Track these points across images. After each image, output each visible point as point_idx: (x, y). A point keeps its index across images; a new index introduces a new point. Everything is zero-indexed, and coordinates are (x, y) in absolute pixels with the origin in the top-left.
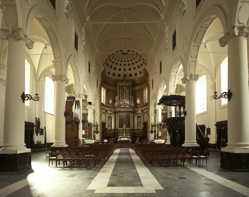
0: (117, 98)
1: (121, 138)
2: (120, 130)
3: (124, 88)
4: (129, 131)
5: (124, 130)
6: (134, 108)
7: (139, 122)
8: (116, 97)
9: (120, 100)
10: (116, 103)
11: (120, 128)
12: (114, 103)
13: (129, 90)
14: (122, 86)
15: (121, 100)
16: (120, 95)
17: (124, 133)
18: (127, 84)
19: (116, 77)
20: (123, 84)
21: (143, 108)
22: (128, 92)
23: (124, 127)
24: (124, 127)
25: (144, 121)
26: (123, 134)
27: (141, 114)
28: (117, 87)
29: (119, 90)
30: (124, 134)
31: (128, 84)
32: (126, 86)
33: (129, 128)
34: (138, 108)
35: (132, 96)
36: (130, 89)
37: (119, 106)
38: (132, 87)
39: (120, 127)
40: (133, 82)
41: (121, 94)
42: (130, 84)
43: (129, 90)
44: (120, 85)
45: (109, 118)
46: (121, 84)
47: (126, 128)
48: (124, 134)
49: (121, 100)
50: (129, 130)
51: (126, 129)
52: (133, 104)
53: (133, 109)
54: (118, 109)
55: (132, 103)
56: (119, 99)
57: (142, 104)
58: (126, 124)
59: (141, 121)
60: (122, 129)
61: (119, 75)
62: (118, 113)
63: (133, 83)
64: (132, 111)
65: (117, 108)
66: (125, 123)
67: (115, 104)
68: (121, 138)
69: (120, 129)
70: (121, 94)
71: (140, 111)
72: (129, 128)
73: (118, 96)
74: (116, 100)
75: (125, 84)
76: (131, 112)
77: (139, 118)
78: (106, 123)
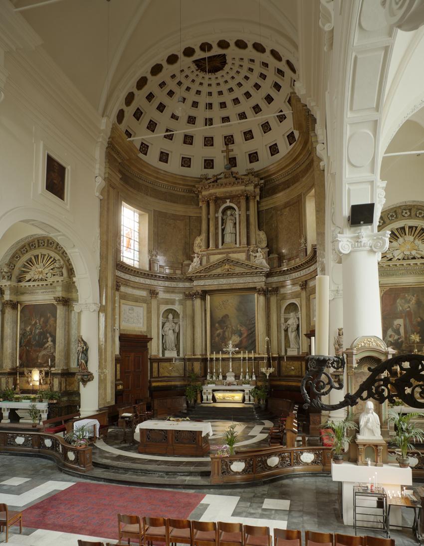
0: (199, 241)
1: (214, 391)
3: (228, 204)
5: (228, 359)
6: (269, 275)
7: (290, 330)
9: (210, 248)
12: (186, 262)
13: (248, 209)
14: (216, 197)
15: (217, 246)
16: (212, 229)
18: (238, 189)
19: (197, 170)
20: (223, 190)
21: (303, 273)
22: (244, 219)
23: (231, 348)
24: (231, 348)
26: (225, 377)
27: (297, 295)
28: (201, 204)
29: (208, 213)
30: (231, 378)
31: (243, 188)
32: (232, 198)
33: (250, 352)
34: (284, 273)
35: (260, 229)
36: (253, 206)
37: (206, 272)
38: (258, 198)
39: (216, 347)
40: (261, 179)
41: (217, 228)
42: (250, 188)
43: (248, 209)
44: (211, 195)
46: (212, 191)
48: (231, 378)
49: (217, 246)
51: (239, 356)
52: (264, 261)
53: (264, 279)
54: (202, 282)
55: (258, 254)
56: (208, 246)
57: (302, 254)
58: (240, 336)
59: (298, 326)
60: (220, 356)
61: (209, 164)
62: (208, 298)
63: (262, 181)
64: (258, 286)
65: (200, 278)
66: (234, 332)
67: (189, 265)
68: (214, 391)
69: (214, 356)
70: (217, 228)
71: (293, 284)
73: (204, 236)
74: (197, 250)
75: (229, 189)
76: (254, 289)
77: (292, 314)
78: (154, 334)
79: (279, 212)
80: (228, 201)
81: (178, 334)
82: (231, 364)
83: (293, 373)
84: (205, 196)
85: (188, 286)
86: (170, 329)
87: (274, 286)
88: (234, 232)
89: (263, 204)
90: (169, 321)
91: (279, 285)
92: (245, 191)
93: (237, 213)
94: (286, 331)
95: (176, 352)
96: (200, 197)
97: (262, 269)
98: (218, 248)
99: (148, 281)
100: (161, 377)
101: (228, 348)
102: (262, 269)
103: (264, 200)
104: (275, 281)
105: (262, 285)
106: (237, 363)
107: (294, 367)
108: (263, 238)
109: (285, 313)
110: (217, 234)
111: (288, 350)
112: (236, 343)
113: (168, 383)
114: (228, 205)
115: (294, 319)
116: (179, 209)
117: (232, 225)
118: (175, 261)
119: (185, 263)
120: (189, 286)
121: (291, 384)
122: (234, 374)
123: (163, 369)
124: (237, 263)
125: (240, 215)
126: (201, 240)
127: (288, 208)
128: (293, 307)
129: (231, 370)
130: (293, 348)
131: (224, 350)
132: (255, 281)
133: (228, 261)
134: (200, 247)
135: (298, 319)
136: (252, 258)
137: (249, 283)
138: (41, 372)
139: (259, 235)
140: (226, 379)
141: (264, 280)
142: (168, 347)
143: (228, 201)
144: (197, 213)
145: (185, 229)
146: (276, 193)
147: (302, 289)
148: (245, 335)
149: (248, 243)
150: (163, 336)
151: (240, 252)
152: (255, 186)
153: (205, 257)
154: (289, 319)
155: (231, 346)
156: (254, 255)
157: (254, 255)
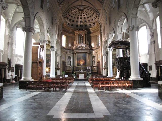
2: (78, 67)
5: (81, 67)
8: (75, 42)
14: (79, 34)
25: (98, 60)
28: (75, 34)
43: (85, 36)
45: (68, 58)
47: (83, 65)
54: (76, 51)
58: (83, 62)
59: (95, 60)
60: (79, 66)
64: (87, 52)
69: (78, 66)
73: (76, 41)
78: (66, 62)
94: (93, 61)
99: (66, 50)
116: (71, 35)
124: (84, 47)
128: (94, 57)
133: (81, 47)
138: (48, 68)
148: (84, 62)
149: (85, 43)
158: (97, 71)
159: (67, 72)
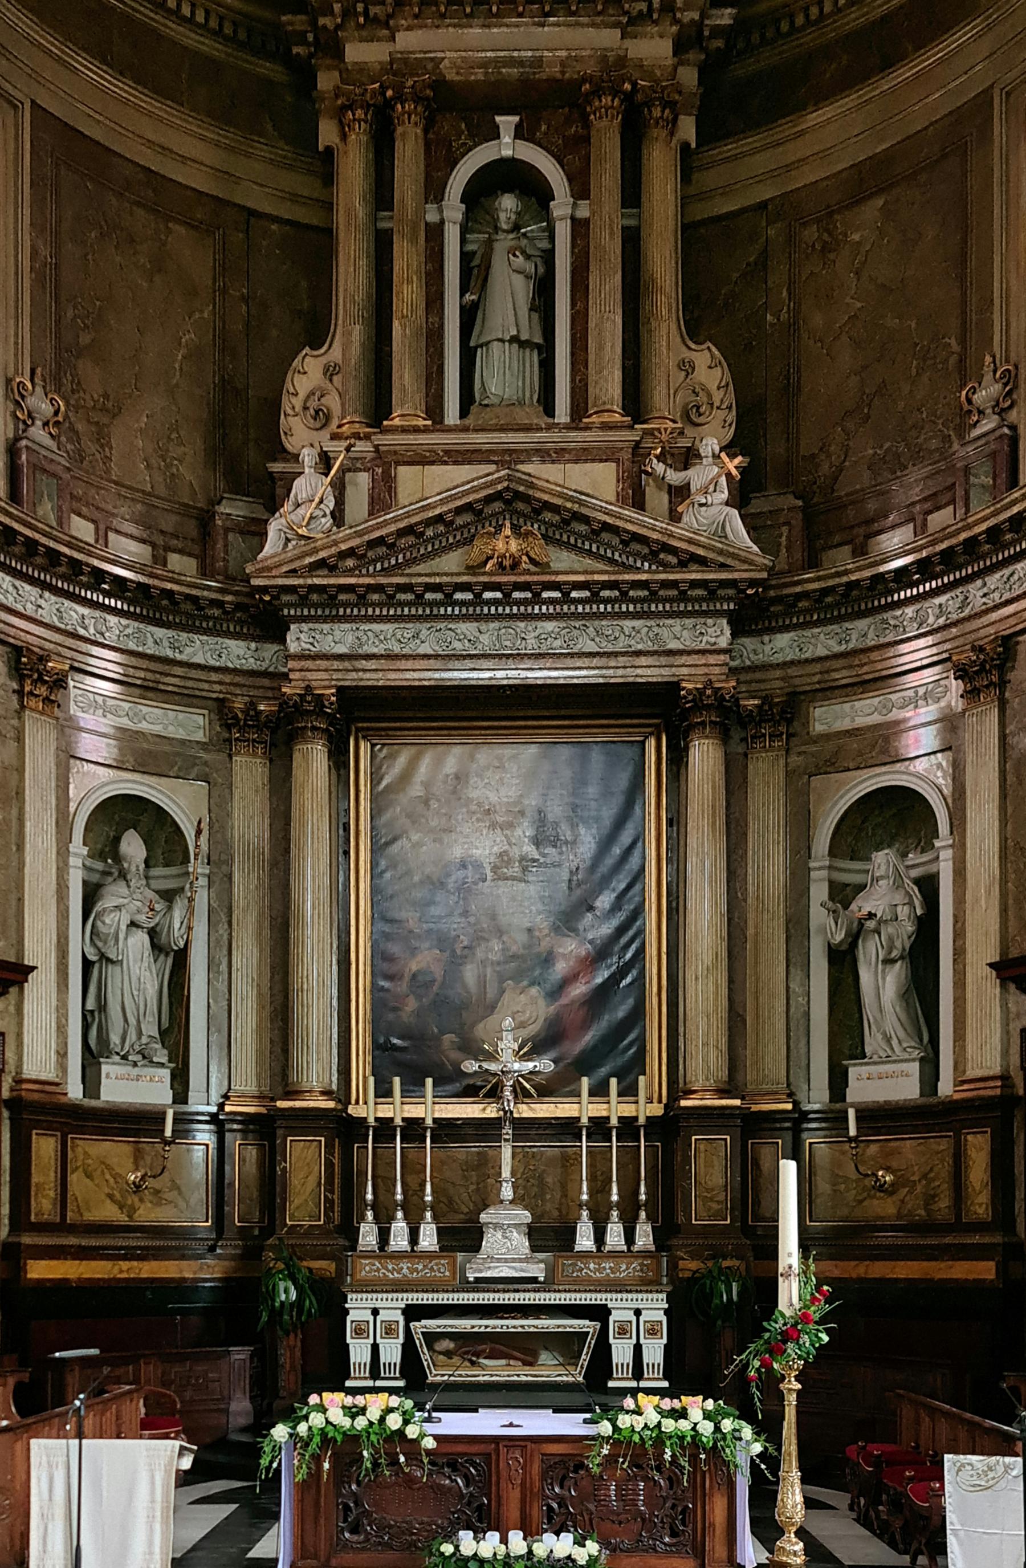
2: (385, 1128)
4: (629, 1158)
7: (869, 952)
10: (301, 487)
11: (384, 1092)
15: (435, 411)
17: (486, 1199)
28: (327, 133)
38: (688, 129)
50: (628, 1125)
53: (719, 632)
55: (698, 476)
70: (434, 301)
72: (628, 1091)
77: (883, 860)
79: (811, 234)
80: (507, 122)
81: (181, 959)
82: (507, 1152)
83: (885, 1208)
84: (362, 68)
85: (237, 664)
86: (133, 924)
87: (775, 683)
88: (538, 339)
89: (709, 179)
90: (123, 875)
91: (811, 681)
92: (622, 61)
93: (561, 206)
95: (165, 1074)
96: (326, 81)
97: (723, 566)
98: (442, 422)
100: (73, 1229)
101: (492, 1057)
102: (723, 566)
103: (729, 148)
104: (779, 658)
105: (715, 668)
106: (549, 1149)
107: (888, 1169)
108: (713, 386)
109: (832, 853)
110: (435, 337)
111: (855, 1072)
112: (533, 1029)
113: (125, 1265)
114: (507, 153)
115: (898, 884)
117: (522, 290)
118: (162, 491)
119: (224, 508)
120: (251, 664)
121: (879, 1269)
122: (525, 1216)
123: (89, 1176)
125: (580, 228)
126: (330, 372)
127: (880, 202)
129: (507, 1192)
130: (888, 1060)
131: (471, 1066)
132: (673, 645)
134: (321, 418)
135: (928, 886)
136: (657, 499)
137: (638, 653)
139: (687, 367)
140: (477, 1248)
141: (723, 642)
142: (115, 1039)
143: (507, 122)
144: (294, 198)
145: (224, 291)
146: (800, 108)
147: (971, 694)
150: (87, 965)
151: (584, 455)
152: (680, 47)
153: (363, 479)
154: (862, 887)
155: (508, 1044)
156: (674, 477)
157: (674, 477)
158: (986, 1270)
159: (38, 1270)
